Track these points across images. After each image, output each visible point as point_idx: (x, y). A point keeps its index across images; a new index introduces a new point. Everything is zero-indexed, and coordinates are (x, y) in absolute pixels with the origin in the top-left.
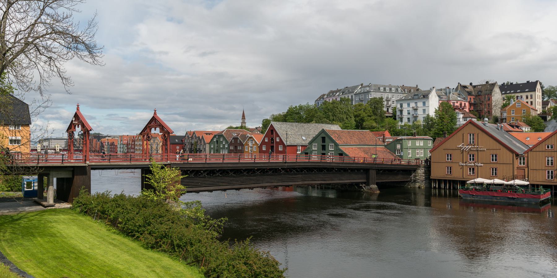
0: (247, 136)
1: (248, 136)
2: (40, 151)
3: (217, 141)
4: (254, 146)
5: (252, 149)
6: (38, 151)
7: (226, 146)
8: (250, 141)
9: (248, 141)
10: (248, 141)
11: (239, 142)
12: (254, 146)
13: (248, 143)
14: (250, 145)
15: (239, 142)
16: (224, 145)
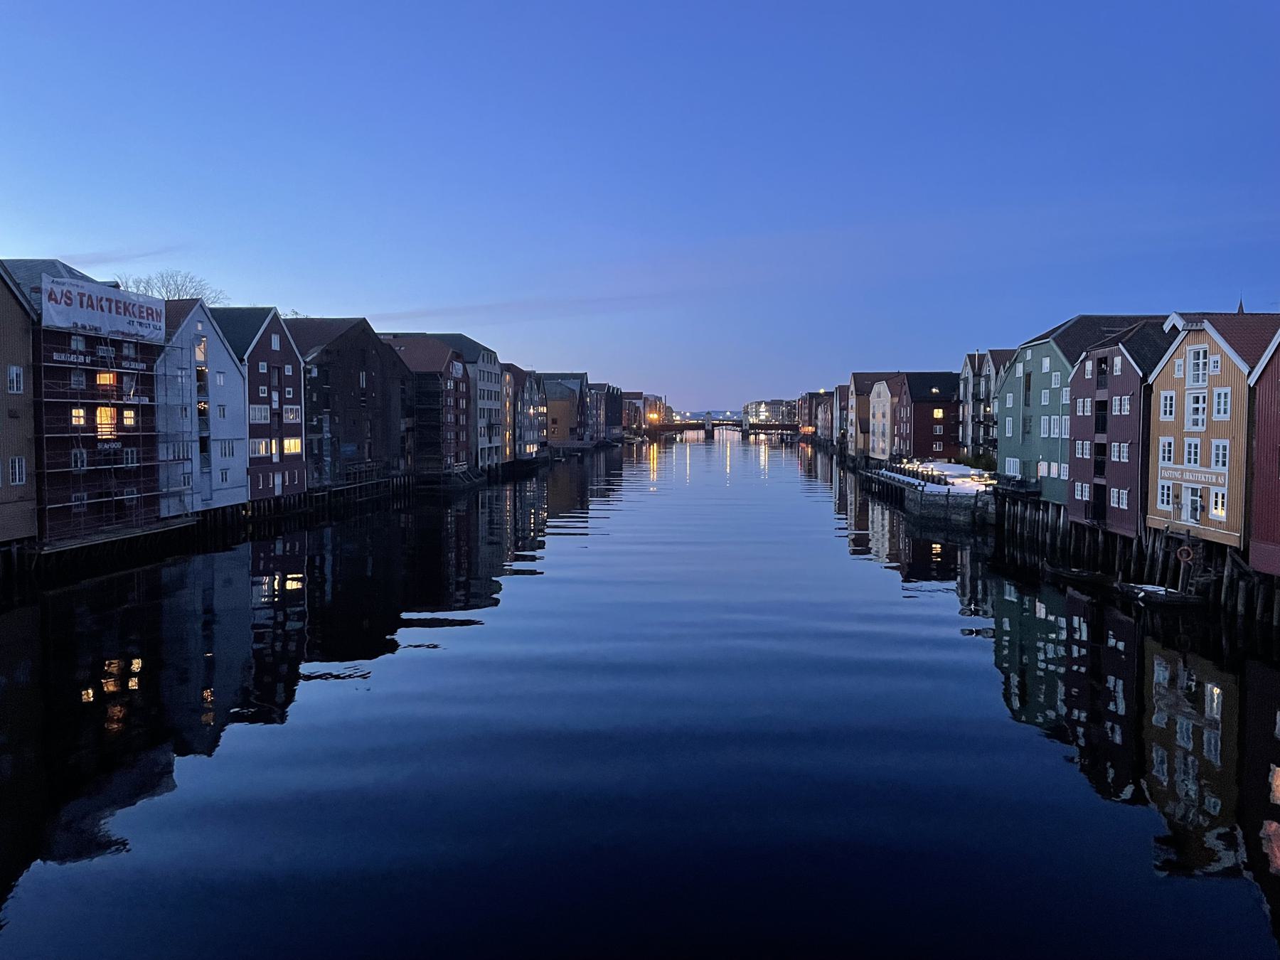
0: (1167, 327)
1: (1174, 327)
2: (710, 428)
3: (1028, 376)
4: (1216, 391)
5: (1201, 405)
6: (707, 427)
7: (1066, 400)
8: (1191, 360)
9: (1179, 362)
10: (1179, 362)
11: (1117, 371)
12: (1216, 391)
13: (1178, 375)
14: (1189, 382)
15: (1117, 371)
16: (1055, 394)
